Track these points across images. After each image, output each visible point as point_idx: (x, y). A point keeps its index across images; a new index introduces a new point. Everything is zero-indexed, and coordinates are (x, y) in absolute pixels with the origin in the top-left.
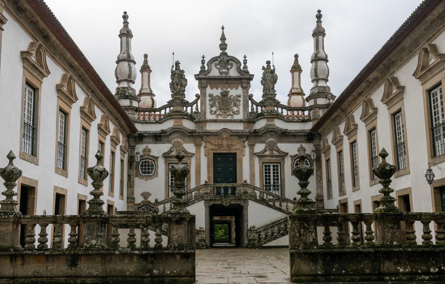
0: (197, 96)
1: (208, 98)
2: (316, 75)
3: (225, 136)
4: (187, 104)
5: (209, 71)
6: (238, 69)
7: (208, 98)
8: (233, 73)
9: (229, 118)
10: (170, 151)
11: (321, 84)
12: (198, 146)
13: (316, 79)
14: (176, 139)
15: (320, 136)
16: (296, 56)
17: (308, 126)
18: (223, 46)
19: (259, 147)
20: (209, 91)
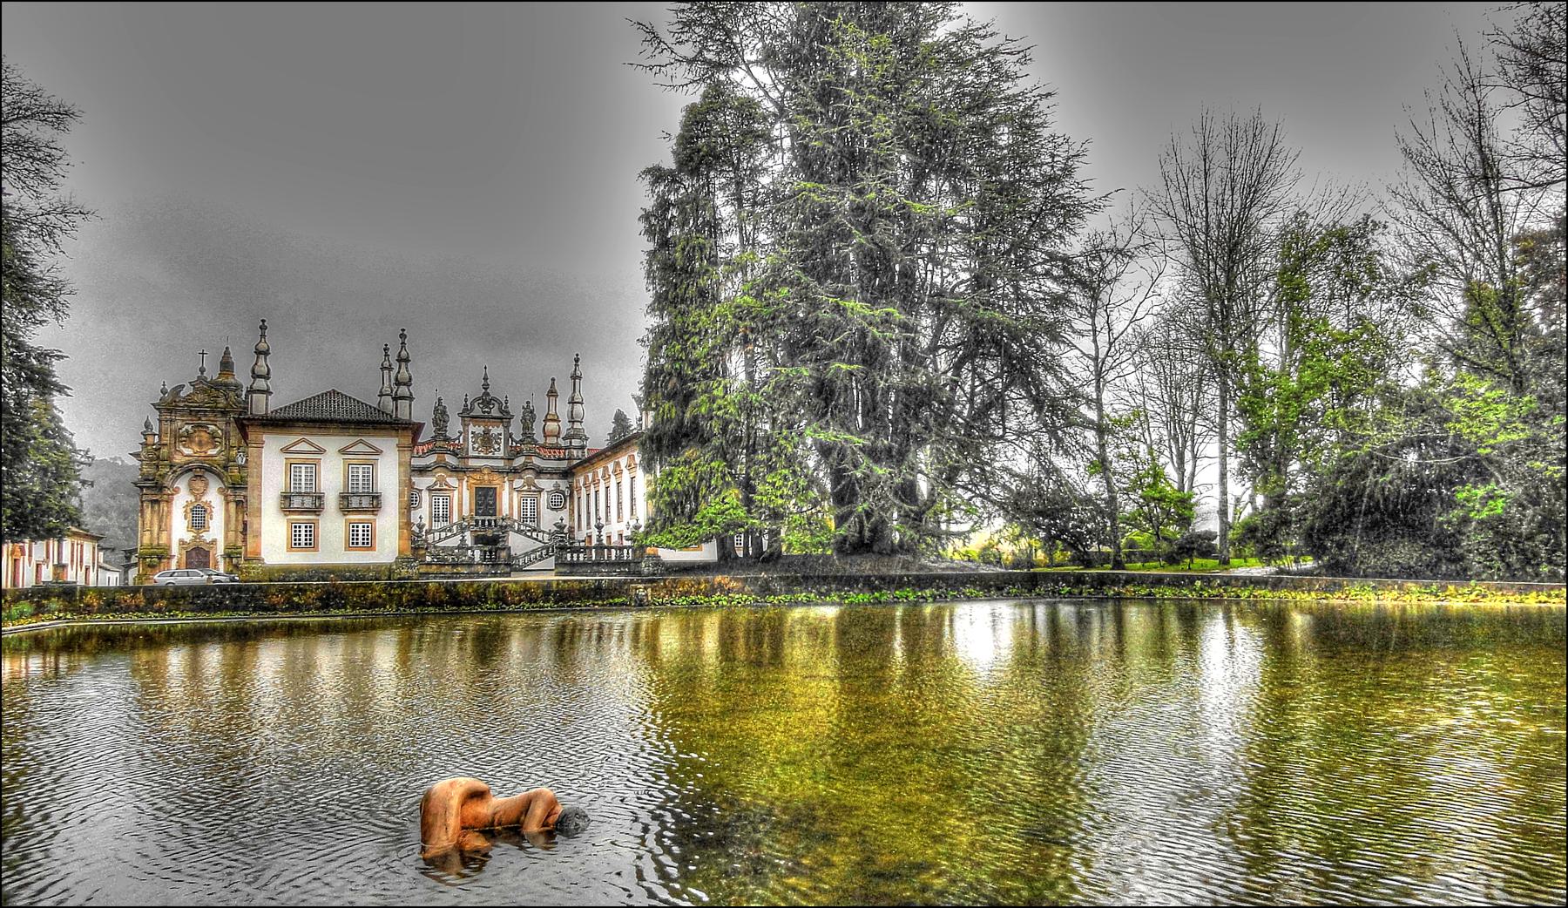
0: (460, 433)
1: (470, 435)
2: (572, 417)
3: (486, 471)
4: (447, 439)
5: (472, 410)
6: (500, 409)
7: (470, 435)
8: (495, 412)
9: (490, 454)
10: (435, 484)
11: (577, 425)
12: (461, 480)
13: (572, 421)
14: (440, 473)
15: (573, 475)
16: (553, 380)
17: (564, 465)
18: (486, 387)
19: (518, 483)
20: (471, 428)
